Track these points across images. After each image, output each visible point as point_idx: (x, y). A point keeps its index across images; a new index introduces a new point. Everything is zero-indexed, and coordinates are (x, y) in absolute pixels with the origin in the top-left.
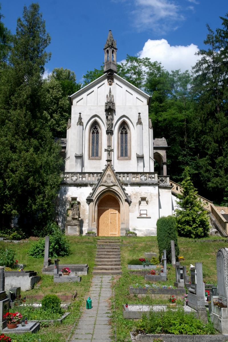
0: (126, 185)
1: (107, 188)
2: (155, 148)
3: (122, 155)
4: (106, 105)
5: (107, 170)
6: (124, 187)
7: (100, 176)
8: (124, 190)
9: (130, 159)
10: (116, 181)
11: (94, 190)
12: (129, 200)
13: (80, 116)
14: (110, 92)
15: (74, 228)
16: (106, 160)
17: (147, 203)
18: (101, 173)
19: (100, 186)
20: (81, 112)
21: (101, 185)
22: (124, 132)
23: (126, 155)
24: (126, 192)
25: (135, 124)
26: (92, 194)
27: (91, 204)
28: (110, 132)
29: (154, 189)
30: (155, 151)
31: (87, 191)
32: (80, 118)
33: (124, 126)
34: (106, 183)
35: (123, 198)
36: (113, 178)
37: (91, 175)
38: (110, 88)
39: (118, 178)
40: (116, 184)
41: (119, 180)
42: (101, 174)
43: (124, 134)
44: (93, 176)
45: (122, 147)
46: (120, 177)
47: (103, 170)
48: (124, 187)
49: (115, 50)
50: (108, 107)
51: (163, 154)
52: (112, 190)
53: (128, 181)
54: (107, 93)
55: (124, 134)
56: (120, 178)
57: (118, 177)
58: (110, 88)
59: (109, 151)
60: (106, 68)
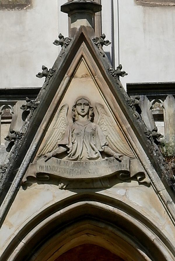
1: (69, 194)
5: (72, 76)
7: (25, 115)
10: (131, 147)
16: (64, 8)
18: (31, 93)
19: (24, 185)
34: (65, 158)
39: (149, 127)
40: (136, 168)
46: (159, 117)
47: (45, 73)
56: (159, 125)
57: (146, 117)
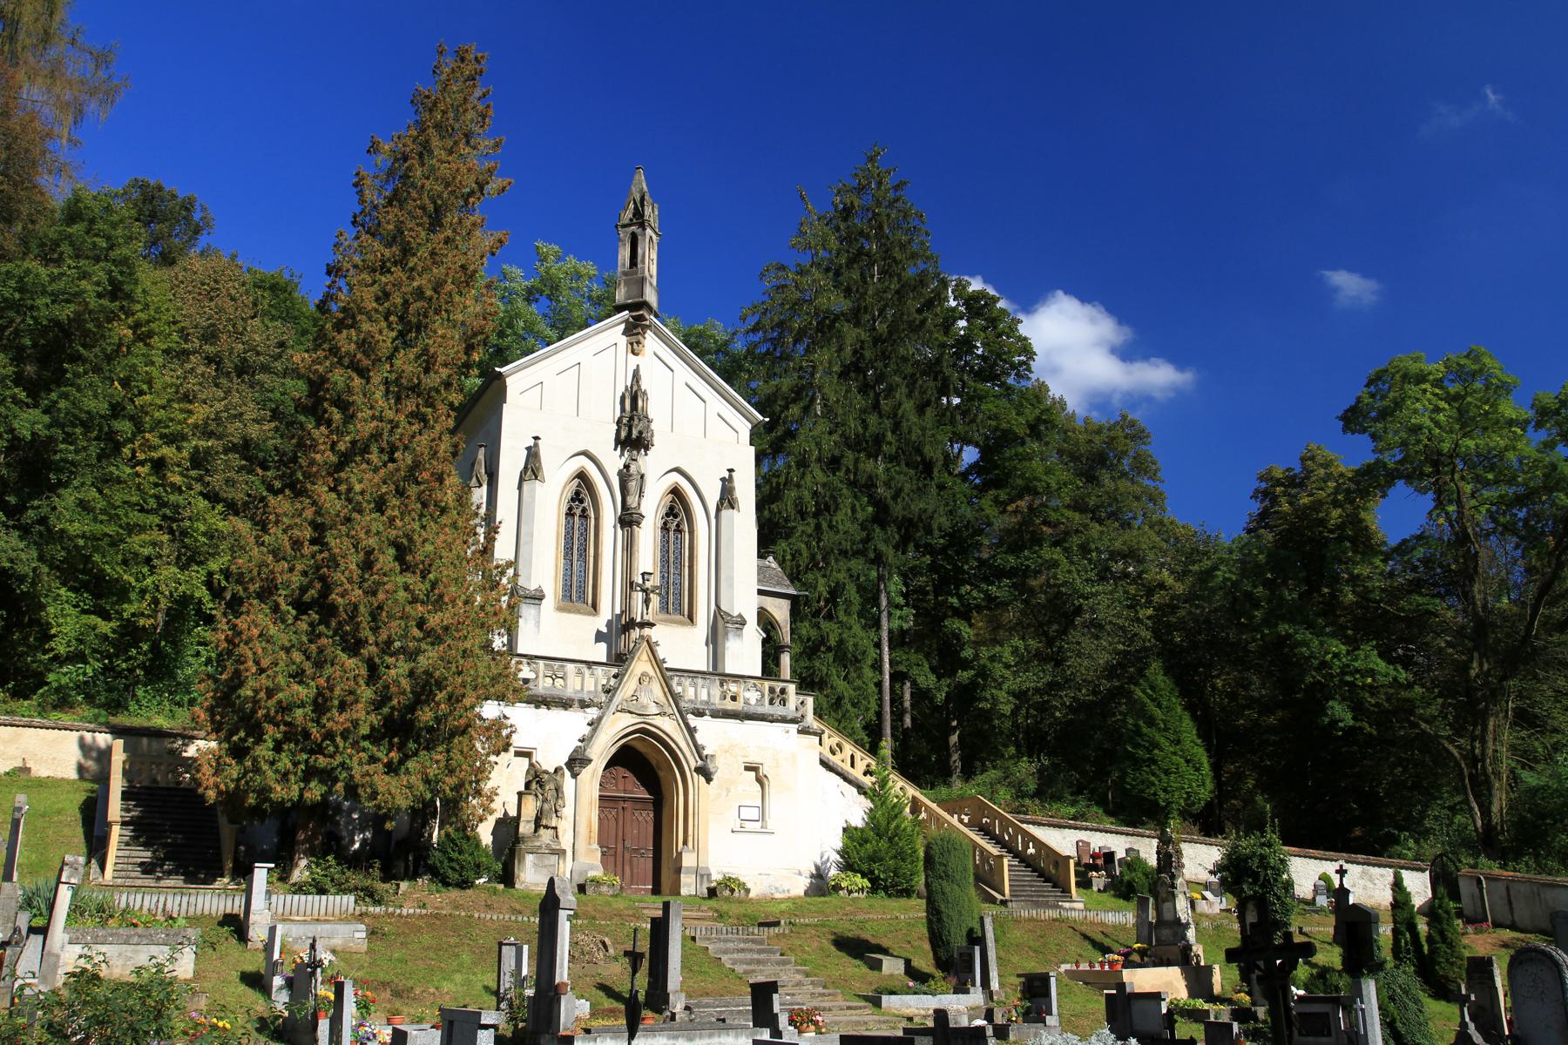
0: (699, 714)
6: (693, 721)
8: (692, 731)
11: (594, 724)
12: (711, 767)
14: (636, 375)
15: (546, 862)
32: (533, 454)
33: (677, 508)
35: (692, 761)
36: (657, 690)
37: (587, 672)
41: (676, 698)
48: (693, 721)
50: (635, 434)
53: (707, 703)
55: (671, 533)
60: (627, 292)
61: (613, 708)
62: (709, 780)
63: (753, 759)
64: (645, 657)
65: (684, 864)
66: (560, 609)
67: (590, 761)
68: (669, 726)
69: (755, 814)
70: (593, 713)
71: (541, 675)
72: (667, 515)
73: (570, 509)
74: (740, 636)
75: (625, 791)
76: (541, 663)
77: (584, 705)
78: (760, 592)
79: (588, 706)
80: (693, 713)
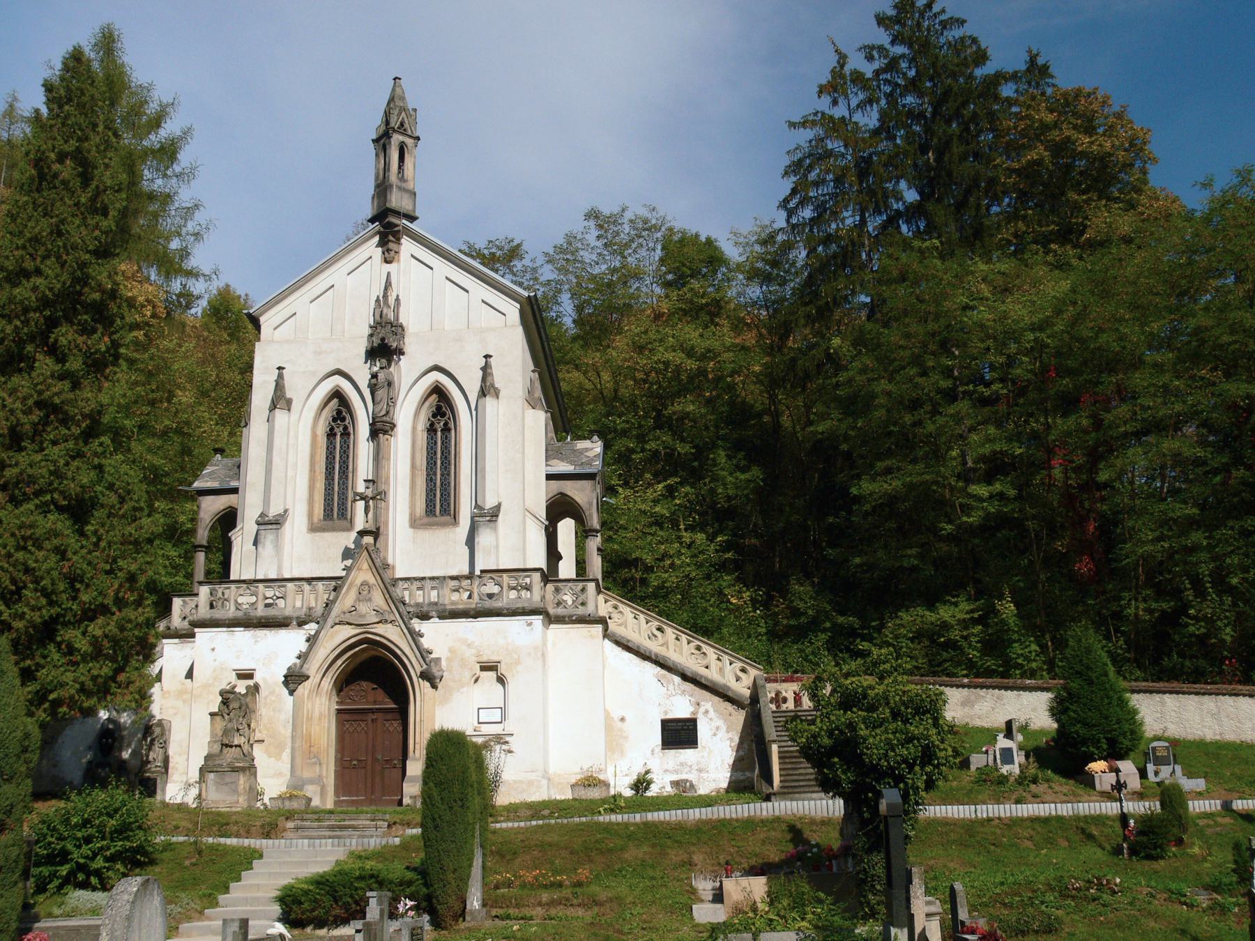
0: (425, 617)
2: (550, 477)
3: (430, 510)
4: (371, 335)
8: (415, 636)
9: (455, 520)
11: (312, 640)
12: (435, 670)
13: (280, 376)
14: (388, 285)
17: (501, 680)
20: (286, 362)
21: (336, 624)
22: (439, 426)
23: (445, 510)
24: (426, 643)
25: (473, 397)
26: (303, 657)
27: (304, 689)
28: (381, 428)
29: (528, 628)
30: (557, 486)
31: (289, 643)
32: (279, 386)
36: (378, 599)
37: (306, 587)
38: (389, 274)
42: (337, 584)
43: (439, 434)
44: (314, 590)
45: (430, 480)
49: (409, 141)
50: (376, 341)
51: (586, 499)
52: (378, 638)
53: (436, 604)
54: (378, 291)
55: (439, 434)
58: (389, 274)
59: (377, 496)
61: (330, 621)
62: (434, 686)
63: (490, 656)
64: (365, 566)
65: (408, 773)
66: (313, 528)
67: (308, 677)
68: (392, 634)
69: (496, 716)
70: (312, 628)
71: (261, 597)
72: (434, 416)
73: (332, 429)
74: (495, 529)
75: (375, 703)
76: (261, 586)
77: (301, 623)
78: (550, 477)
79: (305, 623)
80: (418, 617)
